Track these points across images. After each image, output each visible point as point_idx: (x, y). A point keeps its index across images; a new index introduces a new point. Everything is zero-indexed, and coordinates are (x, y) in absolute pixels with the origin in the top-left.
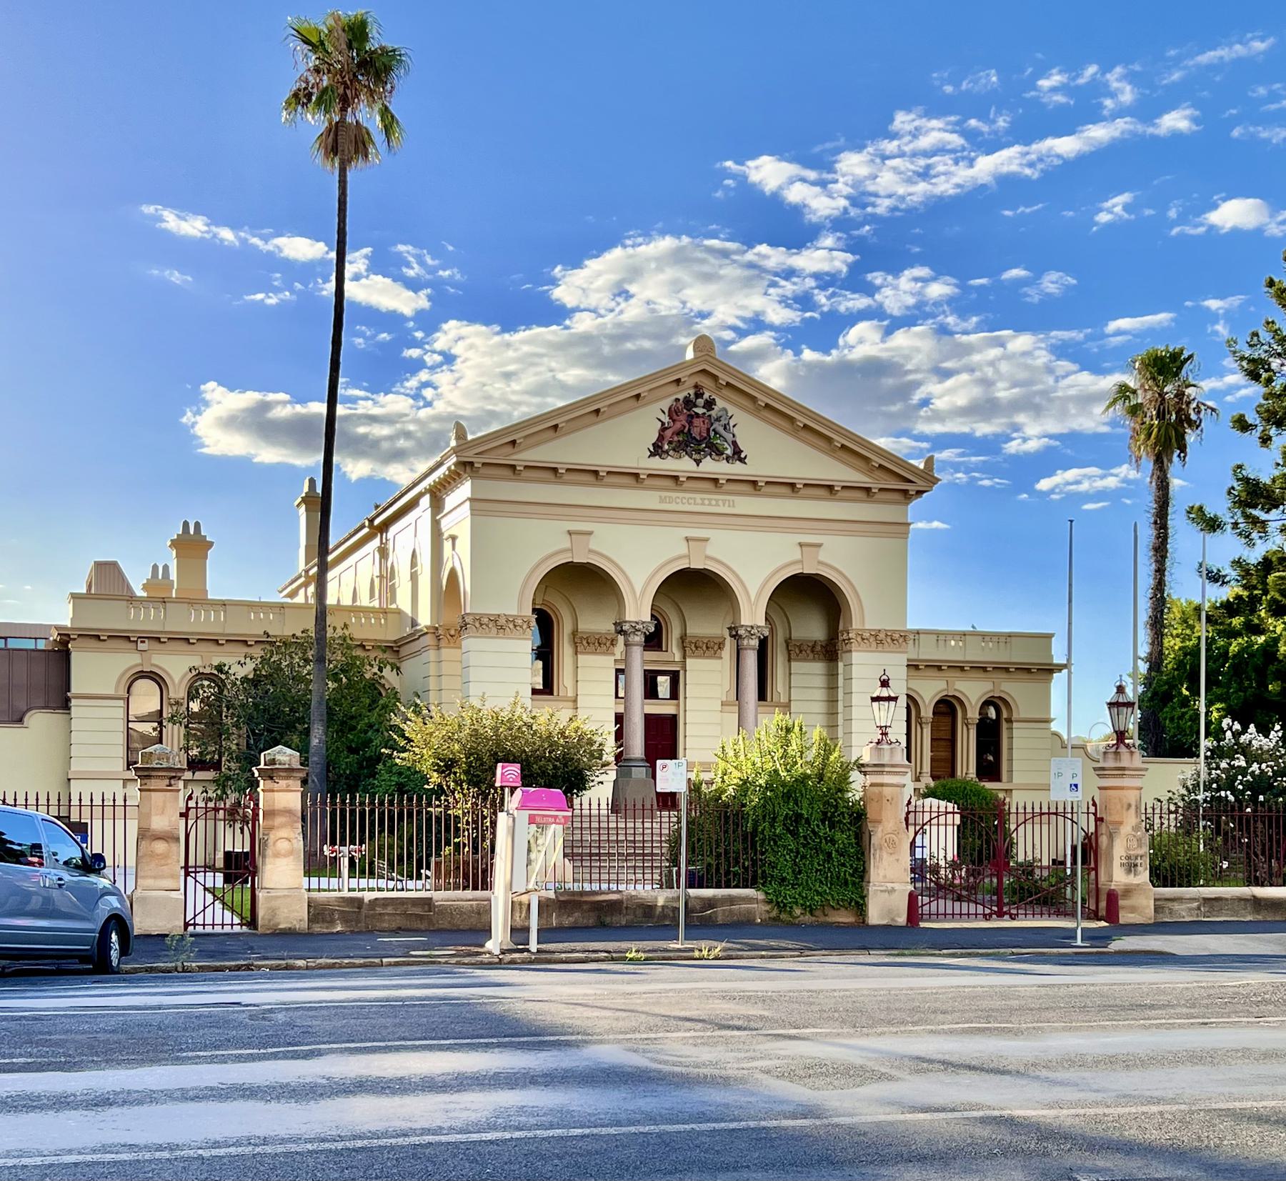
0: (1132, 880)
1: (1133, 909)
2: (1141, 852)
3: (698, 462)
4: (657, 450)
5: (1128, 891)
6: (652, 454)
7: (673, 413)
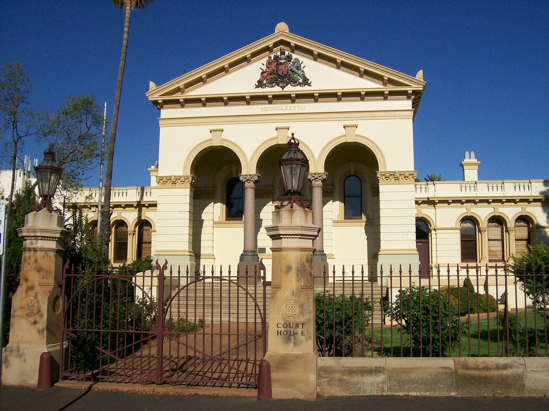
0: (290, 349)
1: (289, 383)
2: (301, 319)
3: (283, 88)
4: (260, 84)
5: (284, 362)
6: (257, 87)
7: (269, 63)
